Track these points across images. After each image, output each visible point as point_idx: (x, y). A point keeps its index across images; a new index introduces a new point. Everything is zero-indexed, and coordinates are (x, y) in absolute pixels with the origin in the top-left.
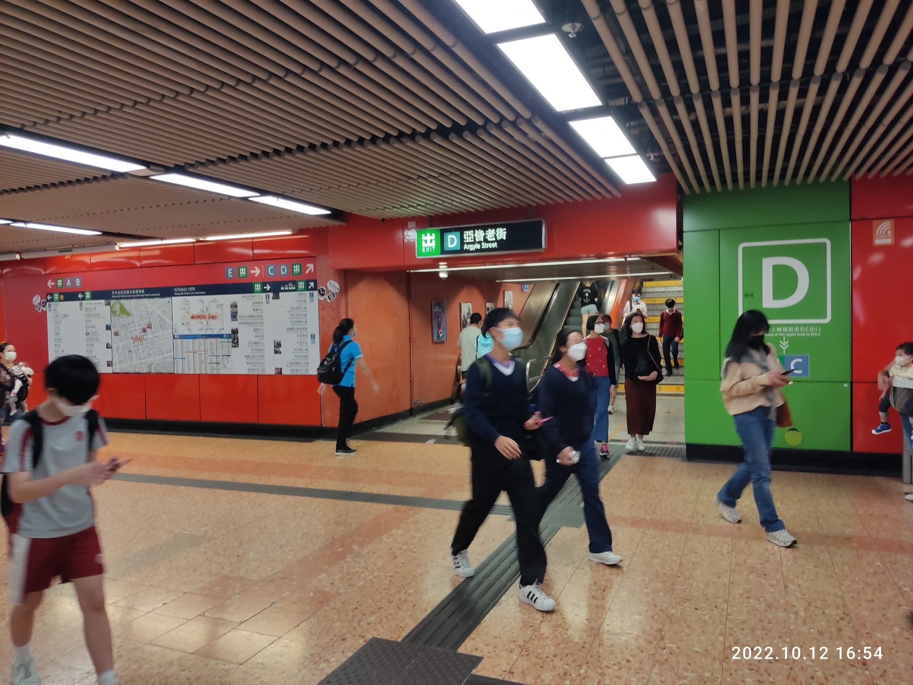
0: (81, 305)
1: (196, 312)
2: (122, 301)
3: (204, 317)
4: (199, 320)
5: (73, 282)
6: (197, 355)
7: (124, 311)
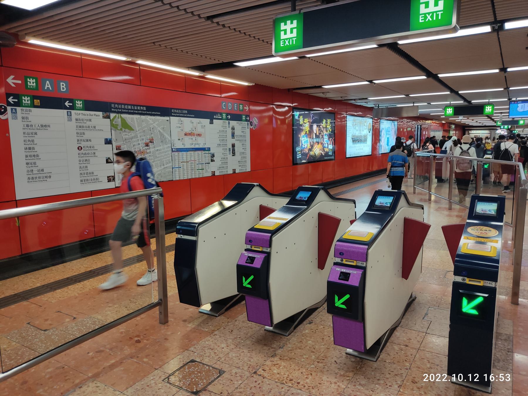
0: (69, 115)
1: (187, 130)
2: (123, 116)
3: (194, 135)
4: (190, 137)
5: (56, 86)
6: (189, 164)
7: (126, 126)
